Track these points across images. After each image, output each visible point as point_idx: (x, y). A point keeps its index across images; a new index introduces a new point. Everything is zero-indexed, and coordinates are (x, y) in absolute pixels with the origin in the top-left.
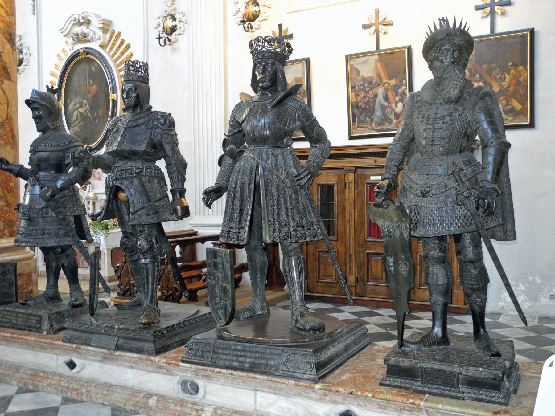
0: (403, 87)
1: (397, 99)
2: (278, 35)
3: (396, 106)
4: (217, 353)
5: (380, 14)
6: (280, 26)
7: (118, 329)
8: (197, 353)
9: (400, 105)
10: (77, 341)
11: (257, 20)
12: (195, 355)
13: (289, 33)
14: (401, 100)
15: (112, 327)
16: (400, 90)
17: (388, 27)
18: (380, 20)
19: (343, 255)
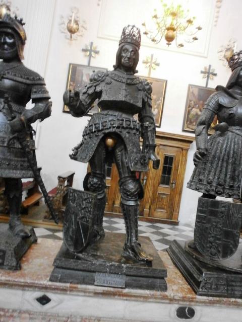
0: (160, 101)
1: (155, 107)
2: (89, 48)
3: (154, 110)
4: (232, 286)
5: (154, 58)
6: (92, 44)
7: (127, 267)
8: (211, 286)
9: (156, 110)
10: (71, 281)
11: (75, 34)
12: (211, 288)
13: (98, 50)
14: (158, 108)
15: (119, 267)
16: (158, 102)
17: (157, 66)
18: (153, 61)
19: (114, 189)
